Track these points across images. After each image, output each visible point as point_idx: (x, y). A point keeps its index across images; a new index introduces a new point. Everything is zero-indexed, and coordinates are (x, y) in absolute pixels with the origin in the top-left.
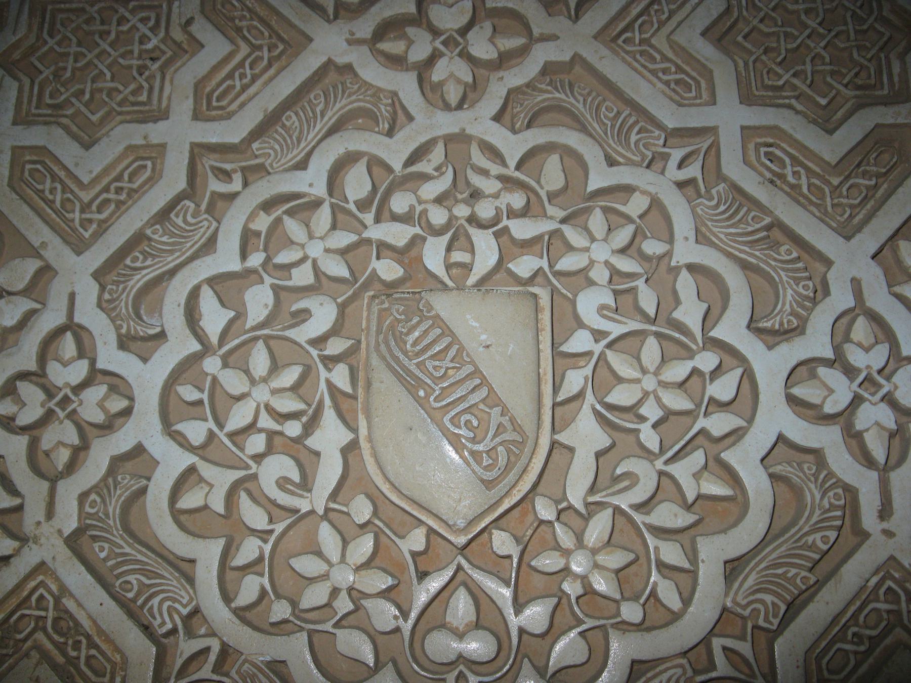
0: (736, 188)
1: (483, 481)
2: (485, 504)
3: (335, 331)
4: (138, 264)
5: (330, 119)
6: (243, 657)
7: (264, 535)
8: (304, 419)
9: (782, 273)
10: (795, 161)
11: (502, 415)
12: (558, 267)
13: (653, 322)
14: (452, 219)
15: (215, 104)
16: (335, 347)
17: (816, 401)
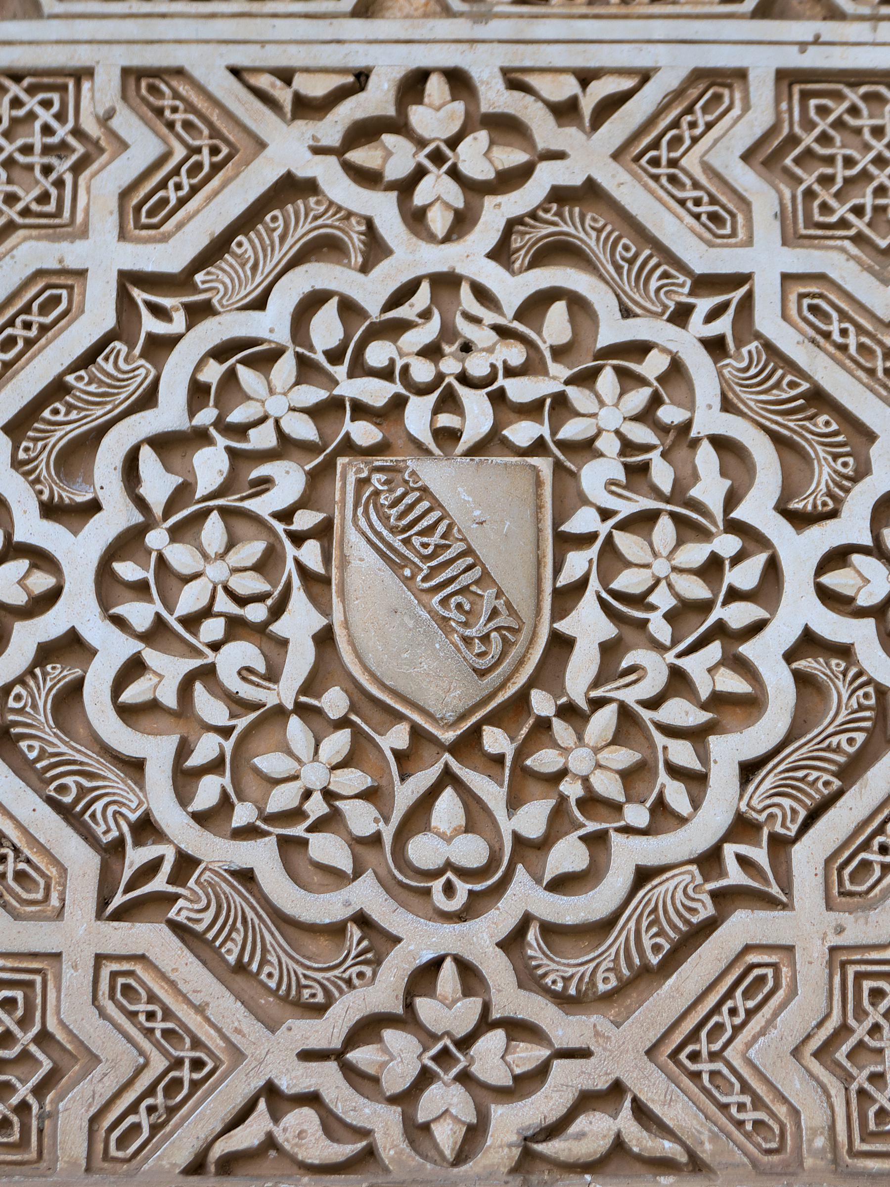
0: (769, 347)
1: (475, 670)
2: (477, 695)
3: (303, 503)
4: (60, 418)
5: (291, 248)
6: (202, 866)
7: (225, 732)
8: (269, 602)
9: (819, 448)
10: (844, 316)
11: (497, 598)
12: (561, 435)
13: (668, 501)
14: (440, 377)
15: (144, 220)
16: (304, 520)
17: (850, 592)
